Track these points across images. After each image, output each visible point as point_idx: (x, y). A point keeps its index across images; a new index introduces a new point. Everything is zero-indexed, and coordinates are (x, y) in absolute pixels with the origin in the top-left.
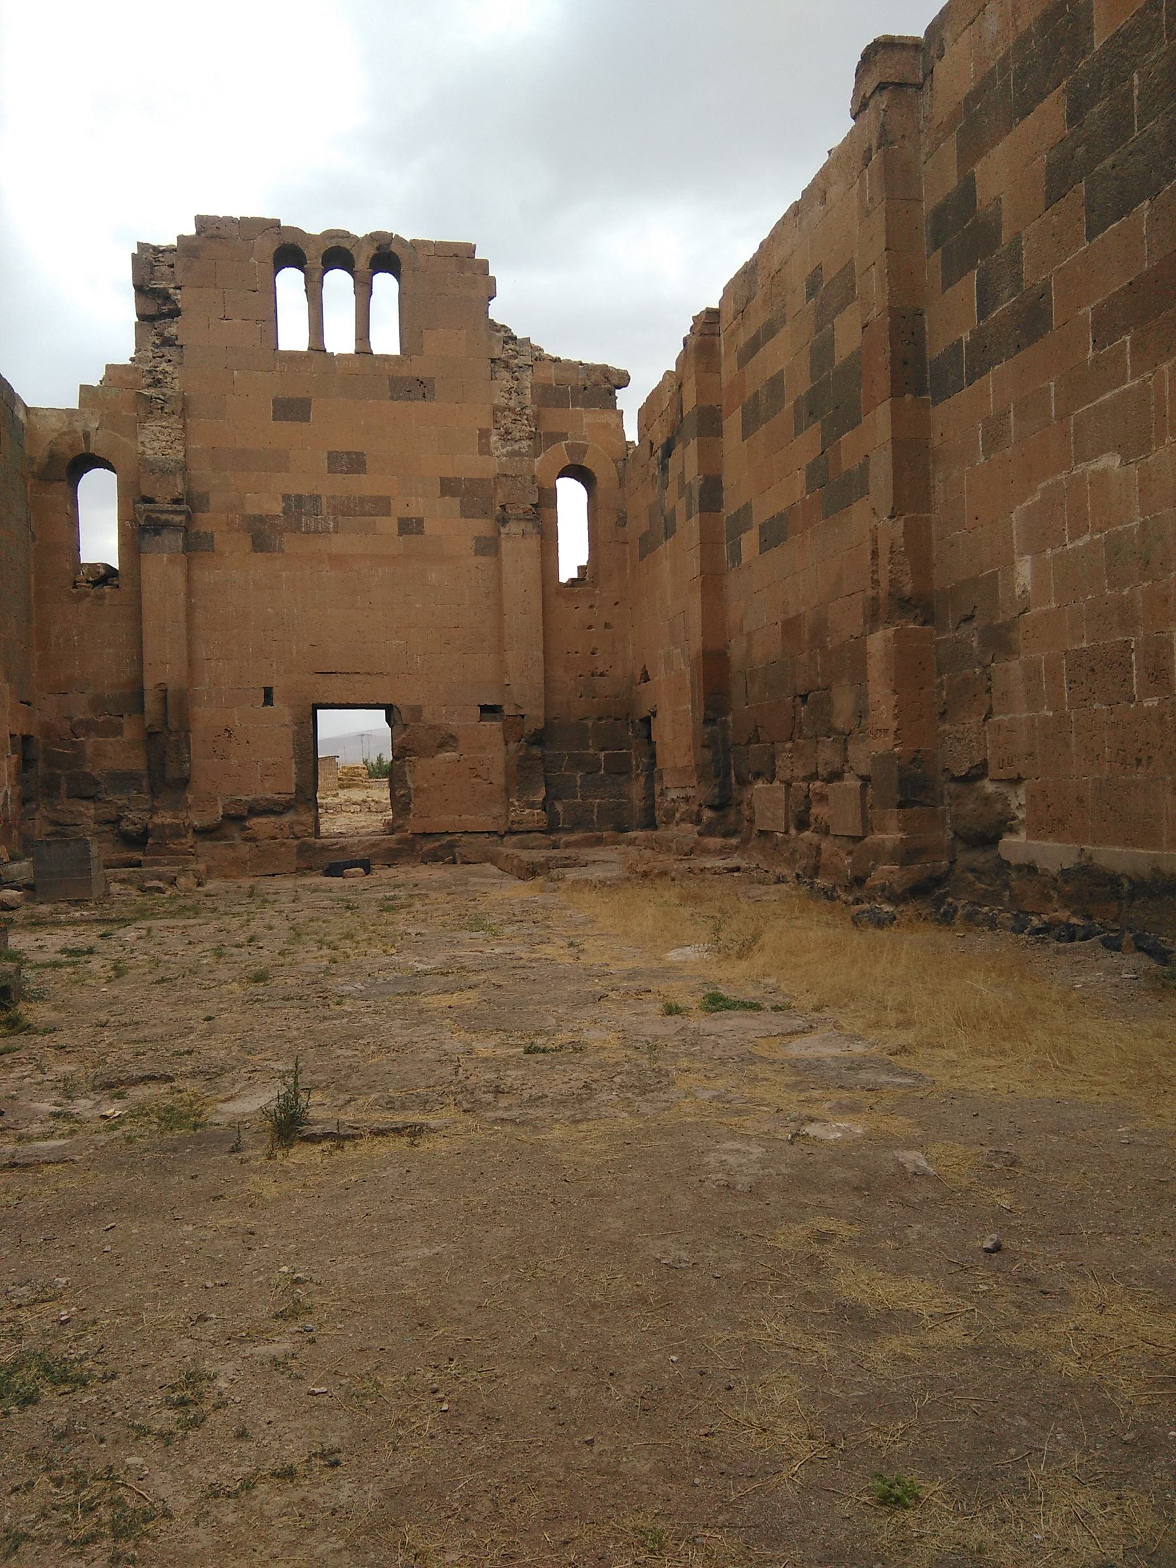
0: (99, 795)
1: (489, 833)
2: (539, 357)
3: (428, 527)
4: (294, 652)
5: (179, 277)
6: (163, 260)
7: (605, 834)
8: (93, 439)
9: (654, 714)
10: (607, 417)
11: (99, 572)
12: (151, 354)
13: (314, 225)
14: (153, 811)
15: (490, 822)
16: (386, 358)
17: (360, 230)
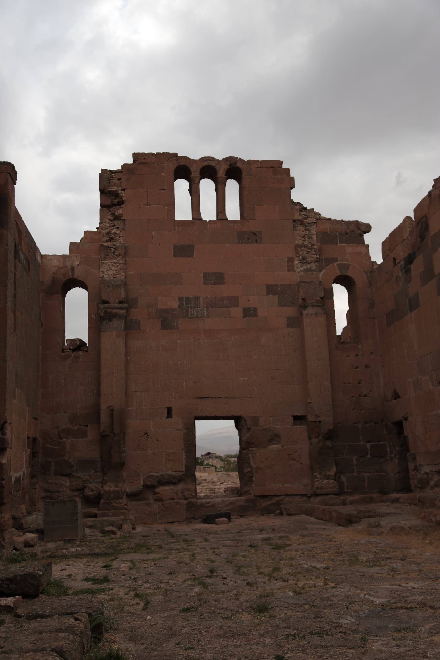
0: (73, 474)
1: (301, 495)
2: (318, 217)
3: (260, 313)
5: (124, 185)
6: (115, 176)
7: (374, 496)
8: (76, 270)
9: (406, 419)
10: (360, 249)
11: (76, 344)
12: (108, 225)
13: (195, 155)
14: (104, 483)
16: (234, 222)
17: (220, 157)
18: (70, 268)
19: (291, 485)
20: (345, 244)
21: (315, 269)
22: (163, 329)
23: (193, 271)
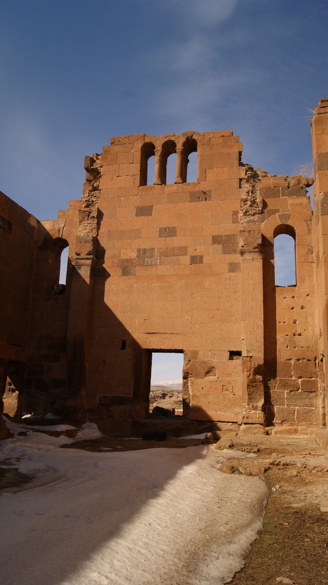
1: (233, 422)
3: (205, 260)
4: (137, 323)
15: (233, 416)
18: (57, 229)
19: (224, 413)
20: (287, 196)
21: (257, 220)
22: (123, 276)
23: (151, 227)
